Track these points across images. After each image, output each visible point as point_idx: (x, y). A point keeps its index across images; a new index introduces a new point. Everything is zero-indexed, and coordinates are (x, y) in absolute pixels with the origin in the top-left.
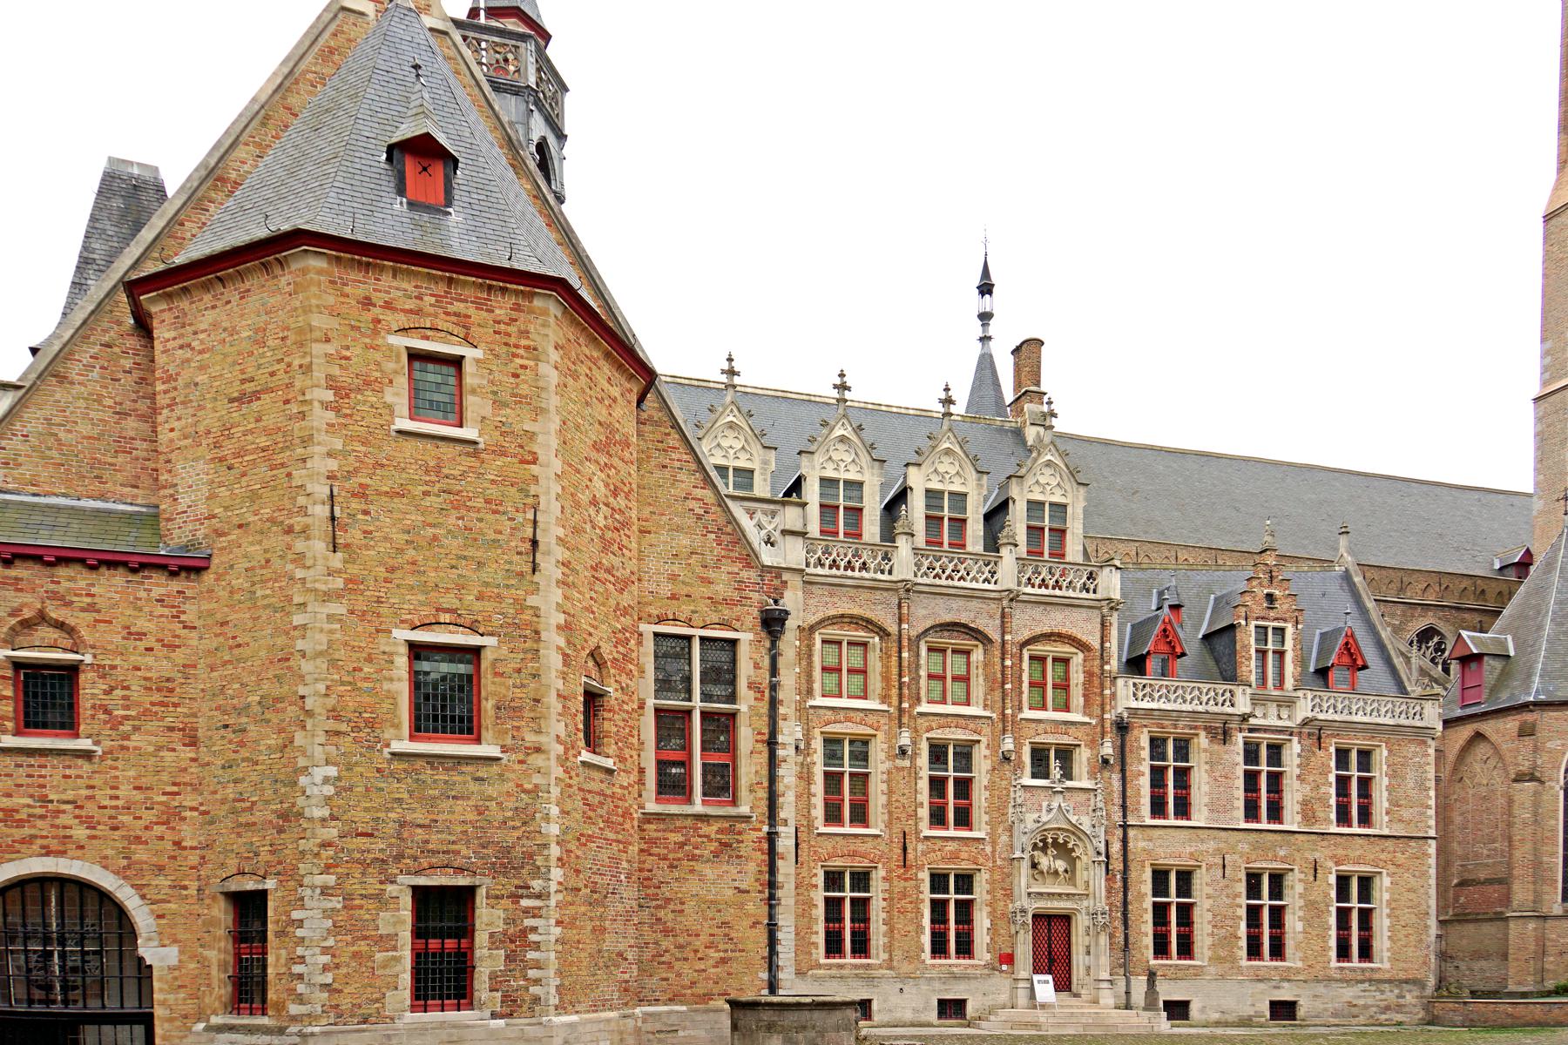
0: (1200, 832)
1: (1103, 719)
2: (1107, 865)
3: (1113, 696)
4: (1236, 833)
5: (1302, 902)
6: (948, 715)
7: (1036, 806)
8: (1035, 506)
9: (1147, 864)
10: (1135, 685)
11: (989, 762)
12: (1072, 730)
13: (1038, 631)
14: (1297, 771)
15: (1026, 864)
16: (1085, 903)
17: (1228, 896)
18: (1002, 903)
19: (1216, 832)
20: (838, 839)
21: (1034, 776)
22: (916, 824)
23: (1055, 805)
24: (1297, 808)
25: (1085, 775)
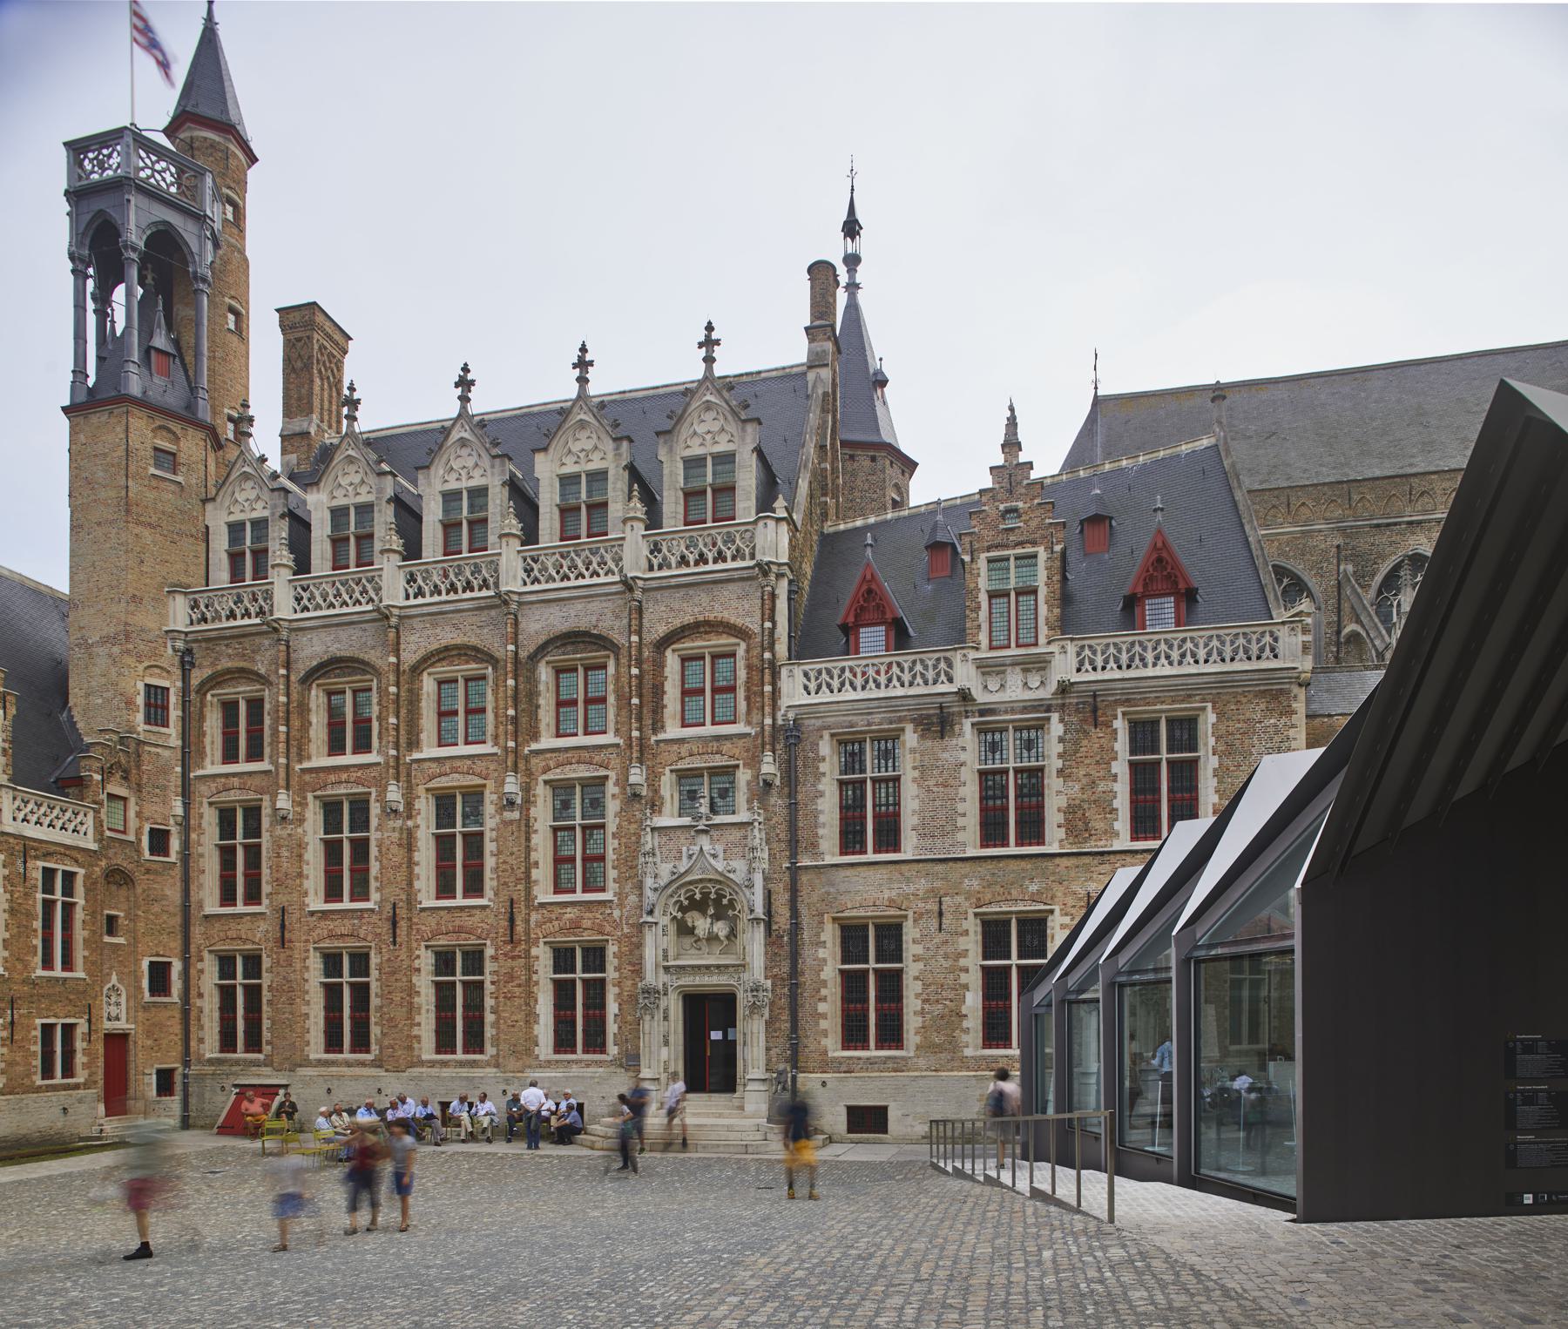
0: (904, 868)
3: (776, 694)
4: (960, 865)
6: (567, 750)
7: (674, 853)
10: (806, 675)
11: (618, 802)
13: (677, 623)
14: (1059, 764)
17: (946, 957)
18: (629, 983)
19: (929, 866)
20: (442, 913)
22: (528, 890)
24: (1060, 818)
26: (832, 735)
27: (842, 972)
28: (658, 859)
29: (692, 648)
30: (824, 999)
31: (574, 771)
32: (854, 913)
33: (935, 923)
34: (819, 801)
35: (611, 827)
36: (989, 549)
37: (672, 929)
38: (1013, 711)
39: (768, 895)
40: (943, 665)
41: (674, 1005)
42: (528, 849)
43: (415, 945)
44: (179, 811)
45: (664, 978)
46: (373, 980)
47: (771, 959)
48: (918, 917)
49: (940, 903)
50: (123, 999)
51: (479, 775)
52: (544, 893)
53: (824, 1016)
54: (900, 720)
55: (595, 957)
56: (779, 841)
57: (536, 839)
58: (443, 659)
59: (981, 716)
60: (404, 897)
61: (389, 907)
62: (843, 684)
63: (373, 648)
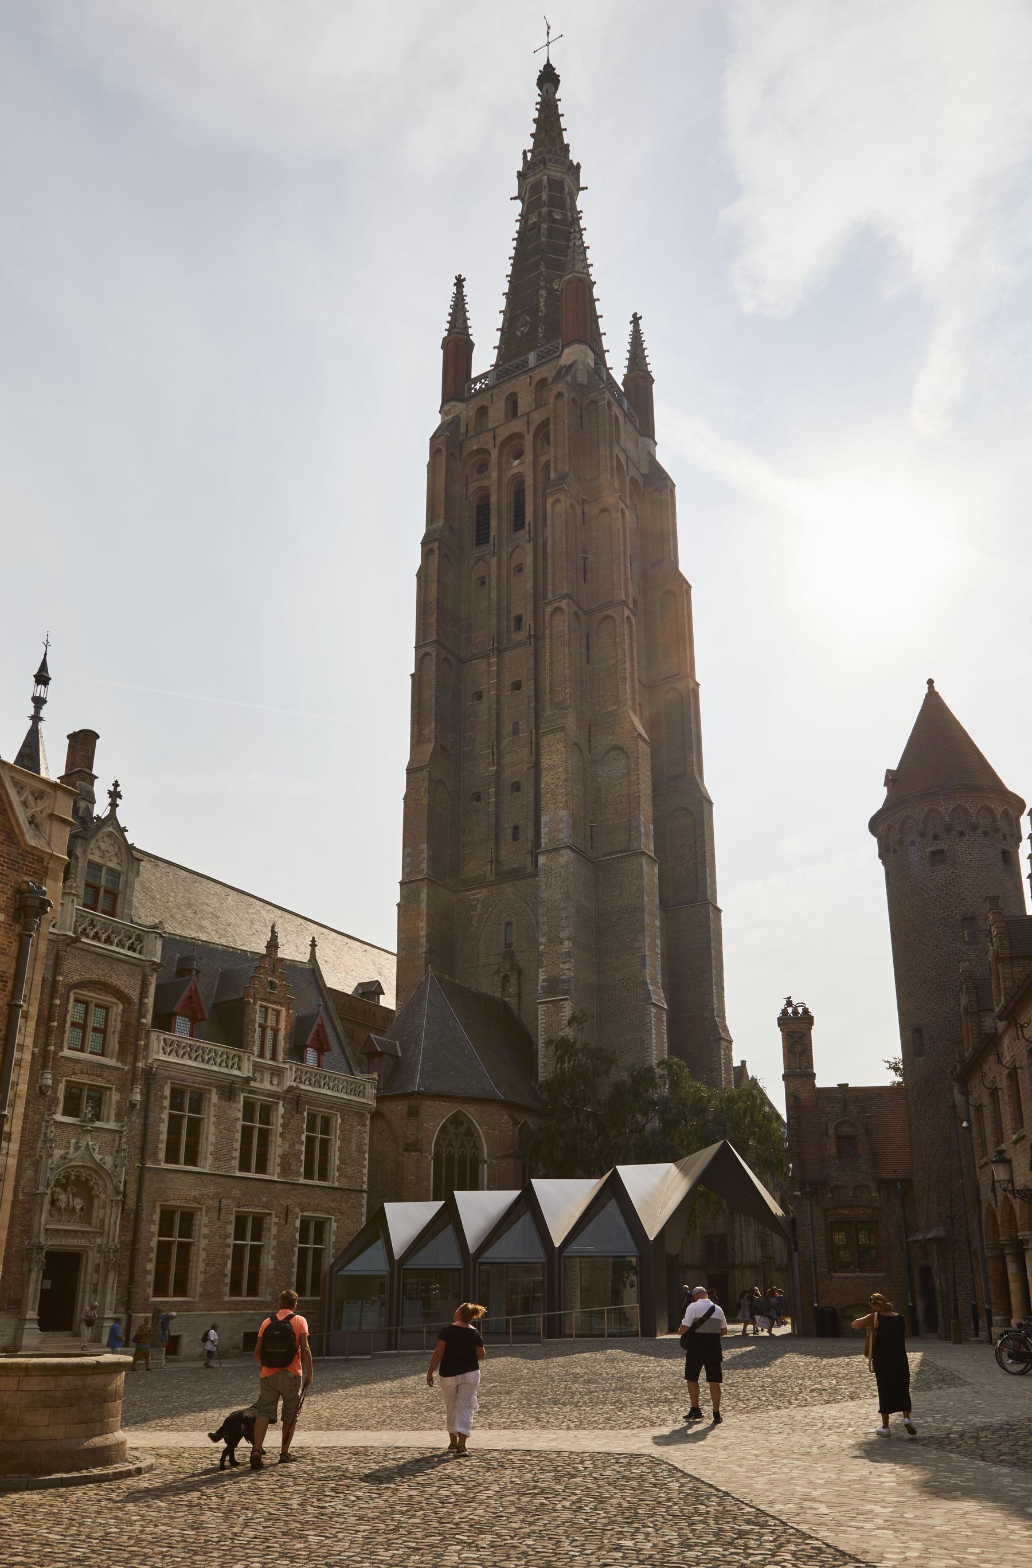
0: (204, 1177)
1: (134, 1068)
2: (124, 1203)
5: (274, 1243)
8: (95, 868)
10: (165, 1040)
12: (106, 1074)
15: (47, 1200)
16: (99, 1241)
21: (65, 1113)
23: (83, 1144)
25: (113, 1117)
26: (172, 1083)
34: (162, 1125)
36: (262, 1000)
38: (263, 1095)
49: (220, 1202)
56: (135, 1147)
59: (249, 1093)
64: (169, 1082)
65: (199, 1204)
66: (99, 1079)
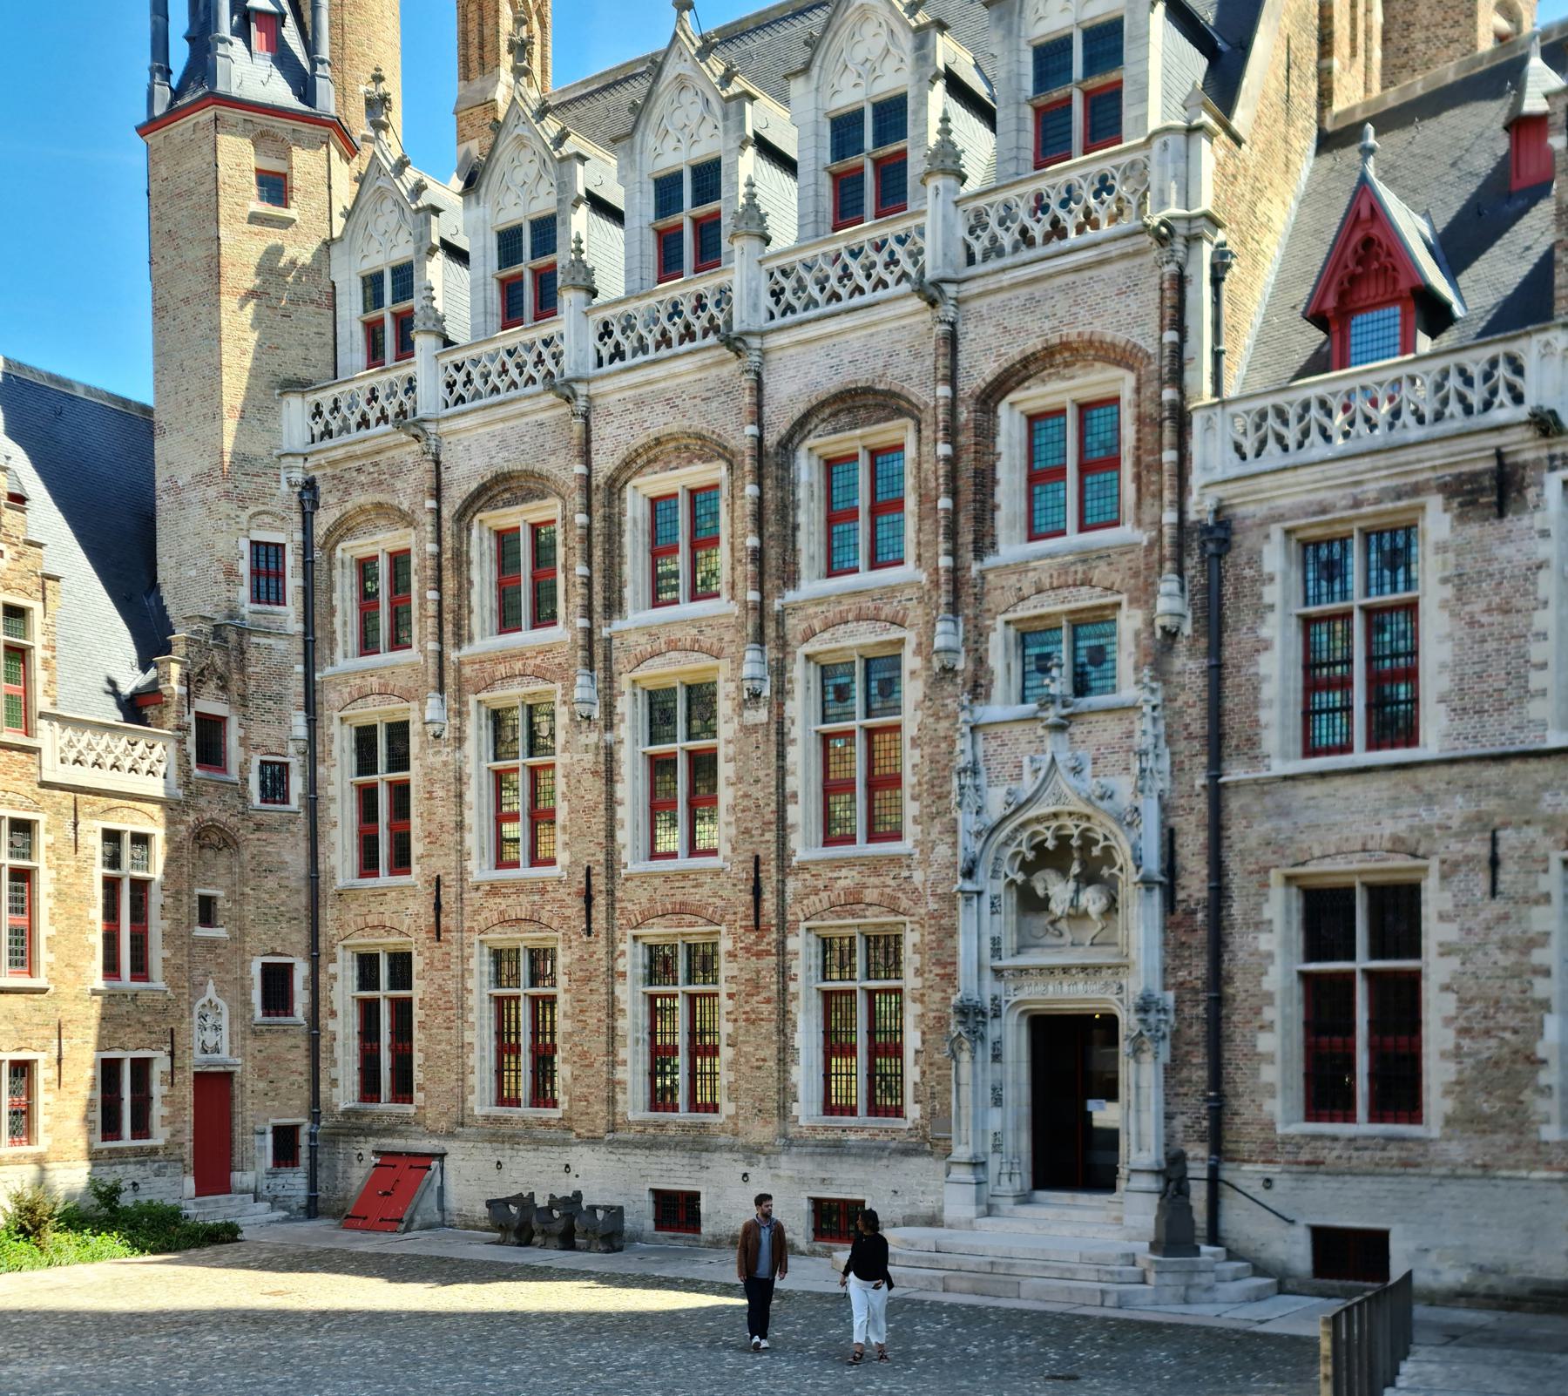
0: (1422, 775)
4: (1533, 765)
9: (1275, 877)
13: (1014, 353)
17: (1505, 946)
18: (938, 996)
19: (1471, 770)
27: (1305, 977)
28: (982, 780)
29: (1043, 396)
30: (1267, 1027)
31: (852, 634)
32: (1326, 866)
33: (1482, 881)
35: (910, 730)
37: (1009, 902)
39: (1170, 838)
40: (1503, 371)
41: (1014, 1038)
42: (782, 772)
43: (618, 934)
44: (301, 730)
45: (990, 988)
46: (562, 991)
47: (1174, 951)
48: (1450, 870)
49: (1494, 841)
50: (224, 1022)
51: (709, 652)
52: (804, 846)
53: (1269, 1058)
54: (1416, 490)
55: (885, 950)
56: (1190, 737)
57: (794, 754)
58: (656, 460)
60: (601, 857)
61: (580, 876)
62: (1306, 433)
63: (553, 452)
64: (1276, 531)
65: (1414, 855)
66: (1084, 589)
